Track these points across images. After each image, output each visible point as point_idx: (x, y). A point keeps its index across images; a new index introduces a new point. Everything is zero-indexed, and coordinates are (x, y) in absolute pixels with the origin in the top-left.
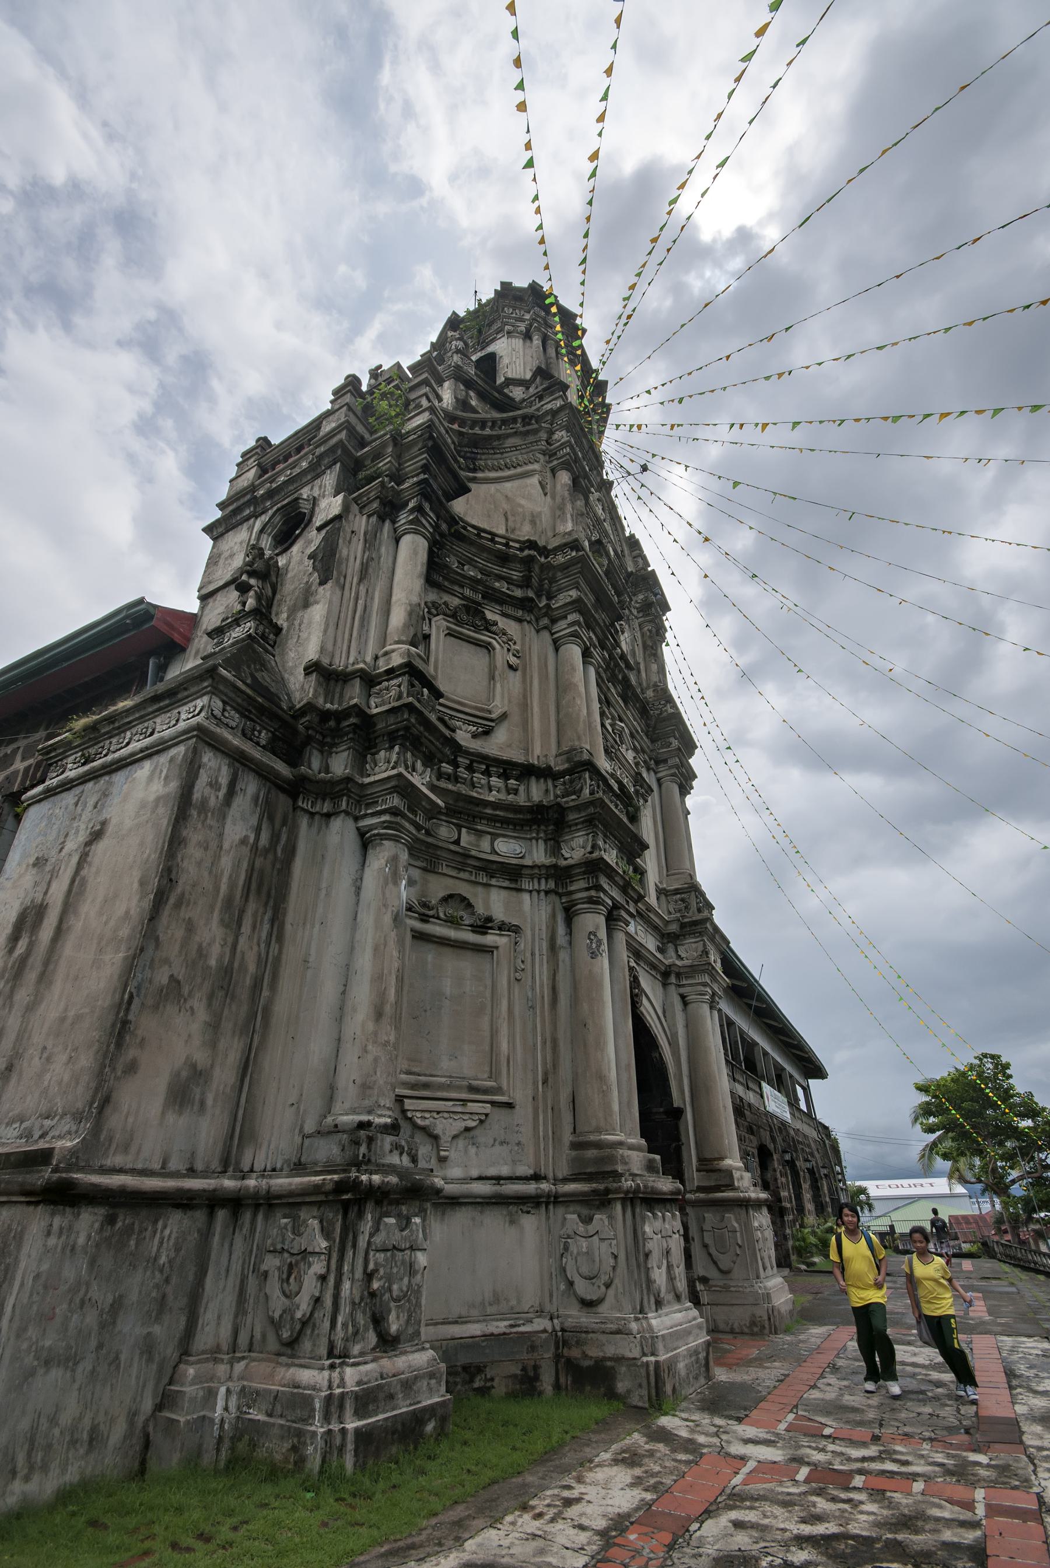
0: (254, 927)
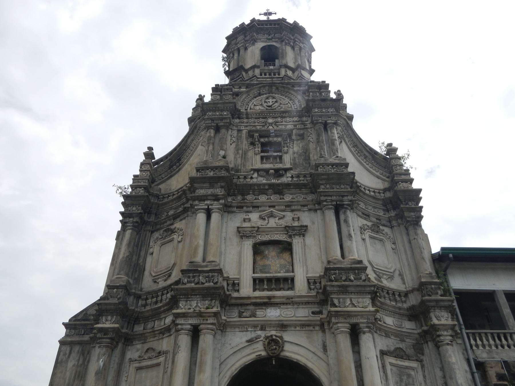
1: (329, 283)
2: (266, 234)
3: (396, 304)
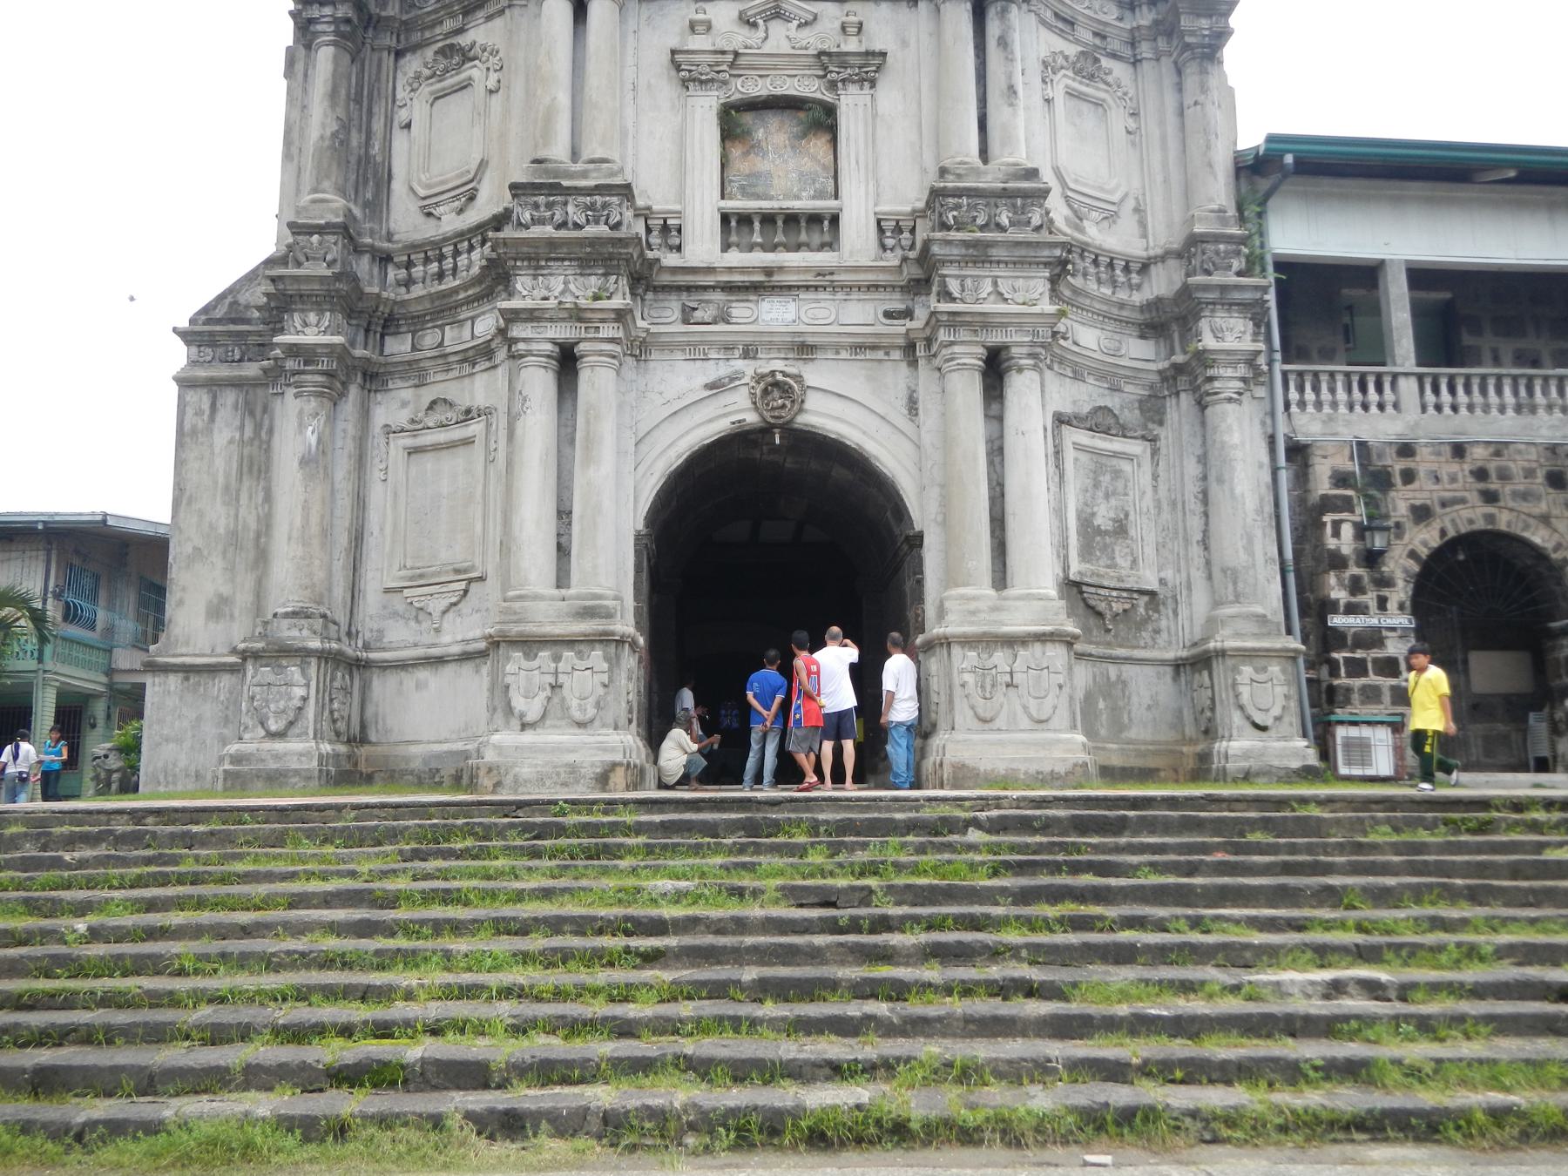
0: (250, 498)
1: (938, 235)
2: (760, 76)
3: (1113, 293)
